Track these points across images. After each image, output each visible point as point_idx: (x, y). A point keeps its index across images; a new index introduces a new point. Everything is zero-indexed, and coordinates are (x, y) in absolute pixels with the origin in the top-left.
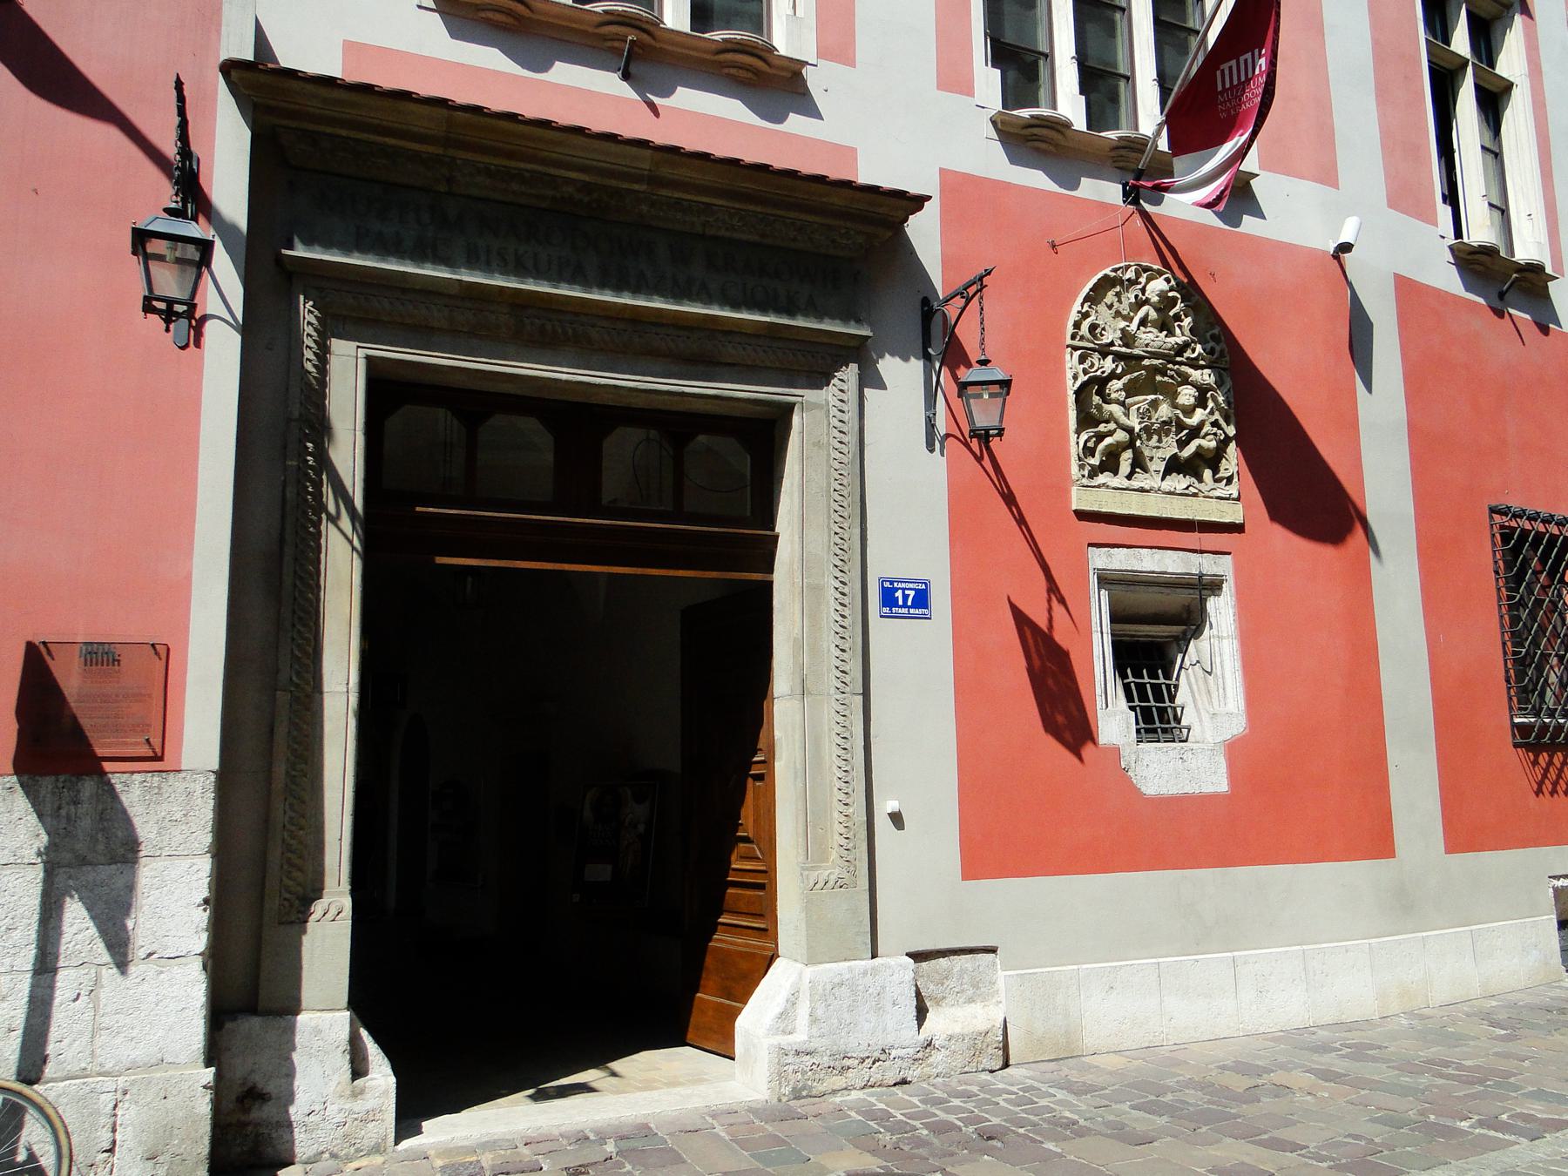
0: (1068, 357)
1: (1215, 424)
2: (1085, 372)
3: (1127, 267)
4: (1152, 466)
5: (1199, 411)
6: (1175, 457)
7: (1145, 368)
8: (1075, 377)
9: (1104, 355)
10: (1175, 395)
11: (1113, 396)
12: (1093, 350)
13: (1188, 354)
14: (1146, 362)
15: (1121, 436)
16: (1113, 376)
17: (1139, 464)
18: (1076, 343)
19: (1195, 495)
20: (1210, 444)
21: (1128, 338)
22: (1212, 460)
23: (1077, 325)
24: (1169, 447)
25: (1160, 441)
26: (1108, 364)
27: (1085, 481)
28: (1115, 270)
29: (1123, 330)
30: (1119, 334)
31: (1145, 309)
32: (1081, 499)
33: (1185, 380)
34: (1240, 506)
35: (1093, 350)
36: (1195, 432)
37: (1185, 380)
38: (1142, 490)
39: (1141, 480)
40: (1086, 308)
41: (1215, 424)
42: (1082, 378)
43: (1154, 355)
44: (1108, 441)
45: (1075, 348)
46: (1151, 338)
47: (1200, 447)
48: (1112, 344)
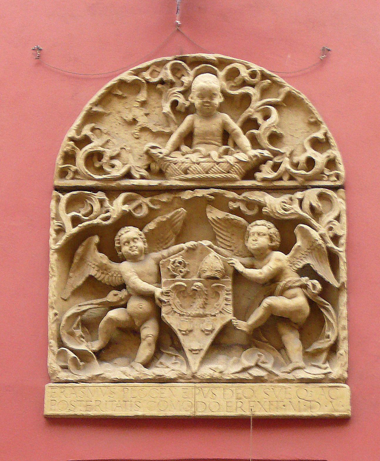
0: (53, 203)
1: (306, 271)
2: (75, 221)
3: (161, 64)
4: (188, 343)
5: (278, 254)
6: (227, 329)
7: (186, 203)
8: (60, 230)
9: (112, 193)
10: (244, 233)
11: (125, 249)
12: (94, 189)
13: (266, 172)
14: (187, 195)
15: (137, 306)
16: (126, 219)
17: (168, 342)
18: (68, 182)
19: (258, 380)
20: (297, 301)
21: (156, 167)
22: (312, 323)
23: (69, 157)
24: (222, 312)
25: (204, 306)
26: (118, 206)
27: (63, 375)
28: (137, 72)
29: (147, 153)
30: (144, 162)
31: (189, 118)
32: (59, 401)
33: (259, 212)
34: (345, 390)
35: (94, 189)
36: (272, 284)
37: (259, 212)
38: (161, 380)
39: (169, 367)
40: (86, 131)
41: (306, 271)
42: (71, 230)
43: (205, 183)
44: (113, 314)
45: (63, 190)
46: (204, 160)
47: (270, 308)
48: (128, 175)
